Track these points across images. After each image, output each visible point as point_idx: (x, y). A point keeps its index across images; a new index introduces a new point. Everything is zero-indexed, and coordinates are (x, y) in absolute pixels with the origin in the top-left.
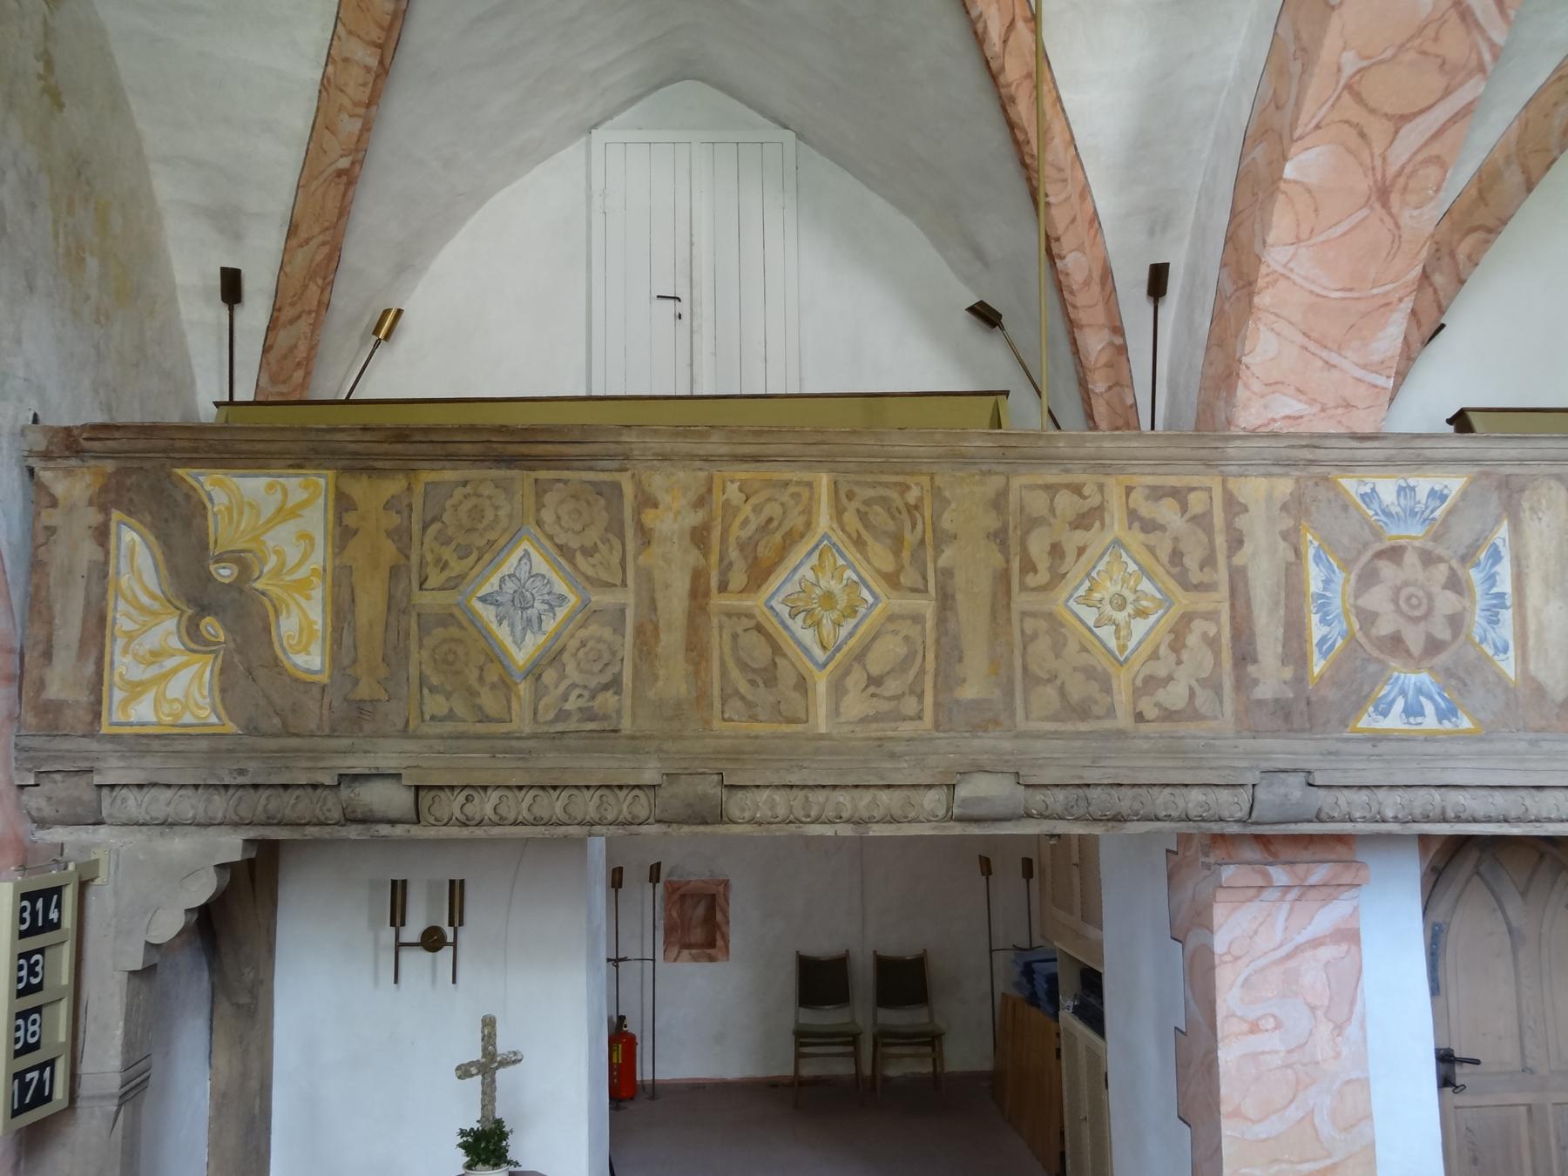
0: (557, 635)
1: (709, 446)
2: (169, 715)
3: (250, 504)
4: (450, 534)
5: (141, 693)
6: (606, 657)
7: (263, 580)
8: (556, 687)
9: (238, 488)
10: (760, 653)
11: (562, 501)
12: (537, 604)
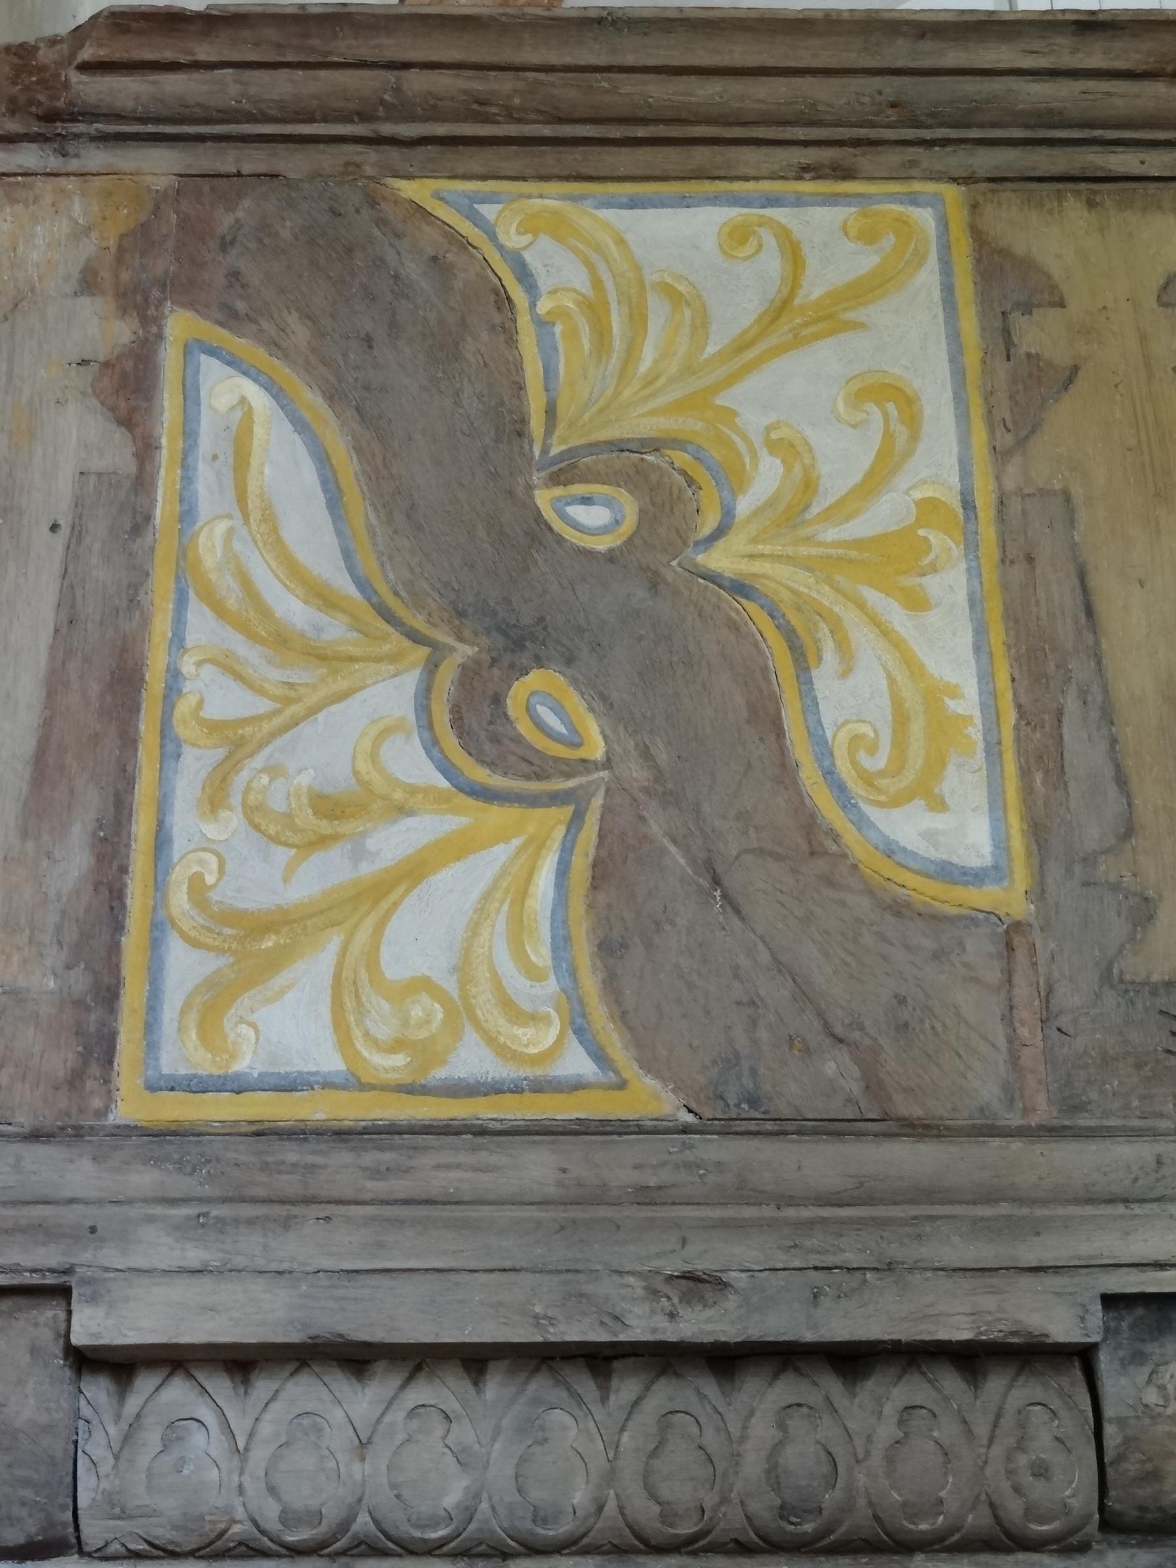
2: (397, 1045)
5: (276, 962)
7: (737, 541)
9: (621, 242)
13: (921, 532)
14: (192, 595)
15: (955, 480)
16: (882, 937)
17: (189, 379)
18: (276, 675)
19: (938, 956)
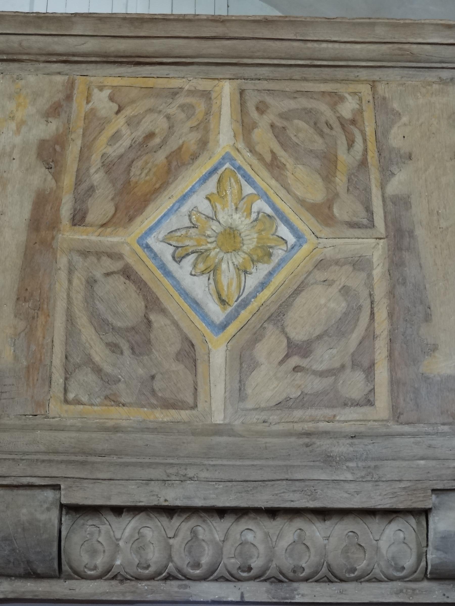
1: (71, 40)
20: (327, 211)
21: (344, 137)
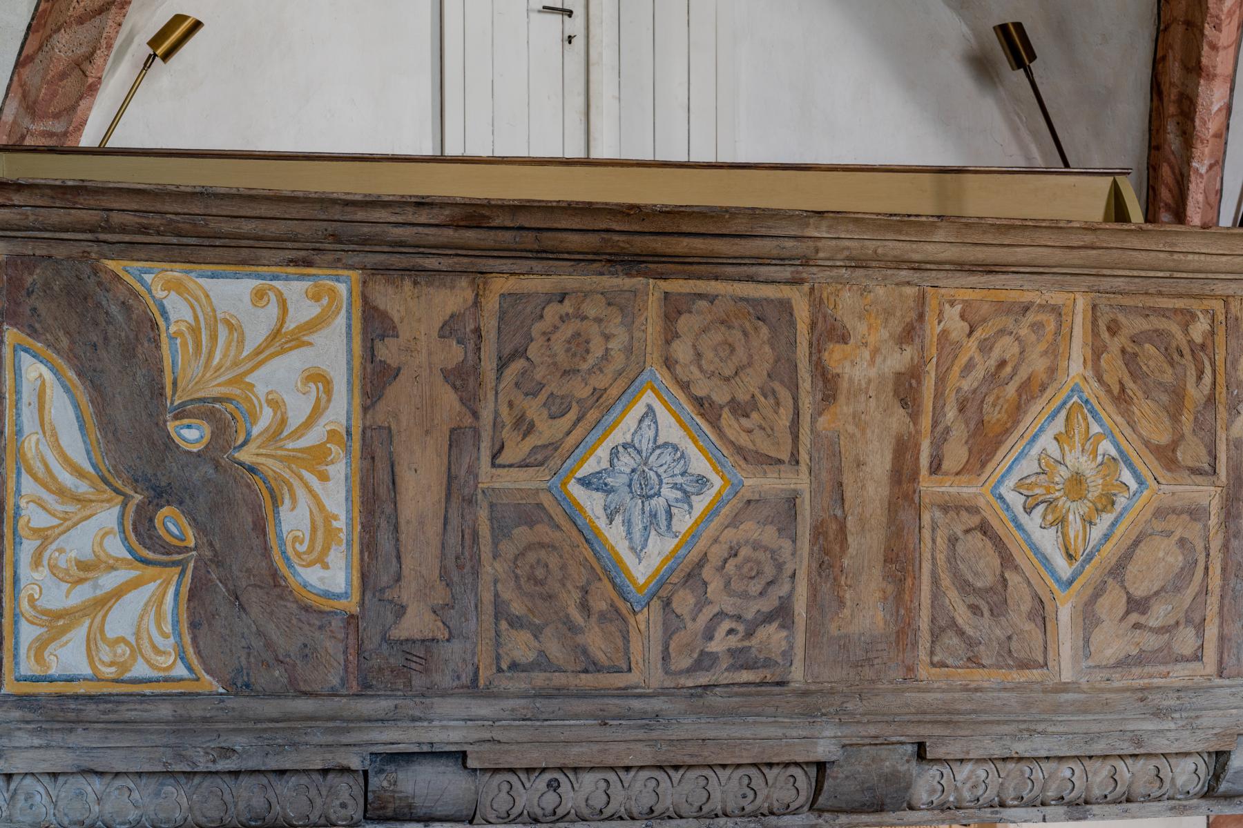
0: (694, 535)
2: (112, 664)
3: (231, 327)
4: (538, 377)
5: (64, 630)
6: (769, 571)
7: (252, 447)
8: (694, 620)
9: (207, 296)
10: (985, 566)
11: (705, 330)
12: (665, 491)
13: (328, 445)
14: (23, 471)
15: (344, 422)
16: (300, 620)
17: (17, 364)
18: (60, 508)
19: (320, 628)
20: (1170, 454)
21: (1193, 367)
